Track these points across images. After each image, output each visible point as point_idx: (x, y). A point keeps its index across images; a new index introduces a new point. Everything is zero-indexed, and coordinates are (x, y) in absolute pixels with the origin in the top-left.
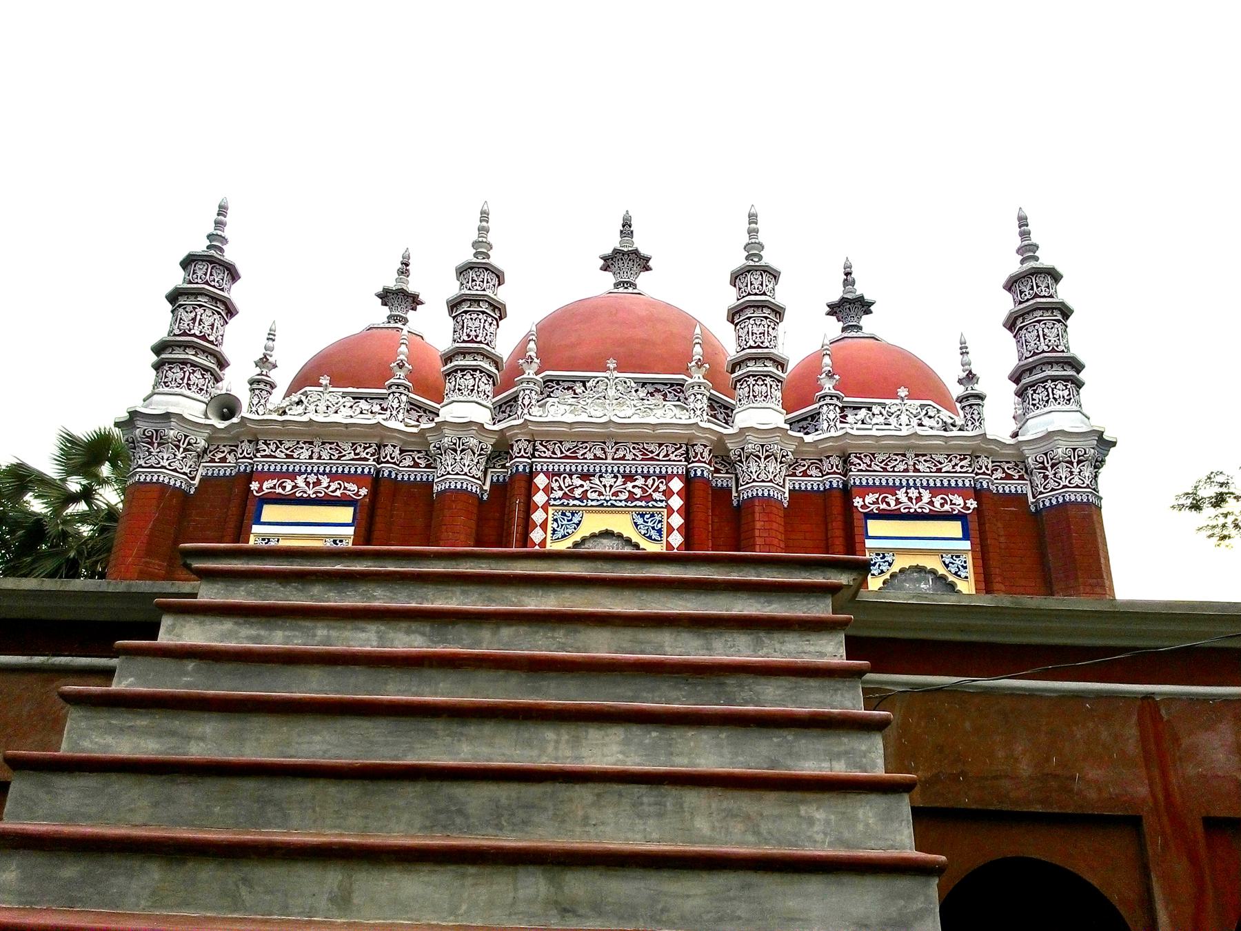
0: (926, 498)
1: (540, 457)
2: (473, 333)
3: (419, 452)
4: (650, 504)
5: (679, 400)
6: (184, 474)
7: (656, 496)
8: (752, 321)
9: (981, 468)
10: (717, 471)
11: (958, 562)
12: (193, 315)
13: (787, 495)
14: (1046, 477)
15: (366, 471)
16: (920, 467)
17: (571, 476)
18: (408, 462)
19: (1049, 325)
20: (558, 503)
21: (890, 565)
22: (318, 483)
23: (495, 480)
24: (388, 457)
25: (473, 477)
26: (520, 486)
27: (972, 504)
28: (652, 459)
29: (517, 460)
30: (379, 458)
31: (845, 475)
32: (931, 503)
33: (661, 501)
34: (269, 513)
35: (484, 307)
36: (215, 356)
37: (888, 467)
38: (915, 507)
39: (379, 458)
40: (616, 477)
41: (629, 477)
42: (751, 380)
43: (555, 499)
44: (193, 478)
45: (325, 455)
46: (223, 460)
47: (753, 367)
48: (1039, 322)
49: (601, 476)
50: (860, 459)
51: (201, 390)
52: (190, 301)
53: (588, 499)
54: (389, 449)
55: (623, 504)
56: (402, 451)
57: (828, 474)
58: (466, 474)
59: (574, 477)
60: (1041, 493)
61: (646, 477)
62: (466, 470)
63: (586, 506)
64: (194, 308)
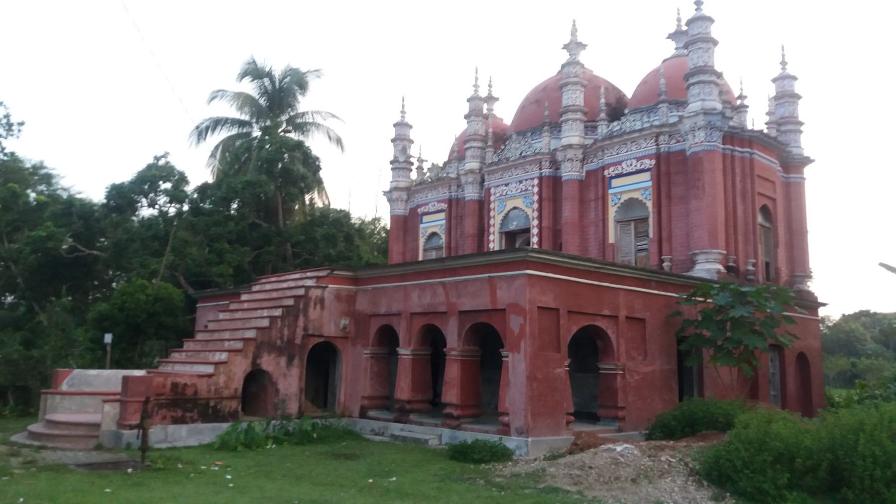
0: (634, 165)
4: (527, 192)
7: (530, 188)
11: (647, 192)
21: (620, 199)
22: (434, 205)
27: (653, 162)
28: (527, 172)
32: (636, 166)
34: (426, 218)
38: (630, 170)
40: (516, 183)
41: (521, 182)
54: (452, 187)
61: (526, 180)
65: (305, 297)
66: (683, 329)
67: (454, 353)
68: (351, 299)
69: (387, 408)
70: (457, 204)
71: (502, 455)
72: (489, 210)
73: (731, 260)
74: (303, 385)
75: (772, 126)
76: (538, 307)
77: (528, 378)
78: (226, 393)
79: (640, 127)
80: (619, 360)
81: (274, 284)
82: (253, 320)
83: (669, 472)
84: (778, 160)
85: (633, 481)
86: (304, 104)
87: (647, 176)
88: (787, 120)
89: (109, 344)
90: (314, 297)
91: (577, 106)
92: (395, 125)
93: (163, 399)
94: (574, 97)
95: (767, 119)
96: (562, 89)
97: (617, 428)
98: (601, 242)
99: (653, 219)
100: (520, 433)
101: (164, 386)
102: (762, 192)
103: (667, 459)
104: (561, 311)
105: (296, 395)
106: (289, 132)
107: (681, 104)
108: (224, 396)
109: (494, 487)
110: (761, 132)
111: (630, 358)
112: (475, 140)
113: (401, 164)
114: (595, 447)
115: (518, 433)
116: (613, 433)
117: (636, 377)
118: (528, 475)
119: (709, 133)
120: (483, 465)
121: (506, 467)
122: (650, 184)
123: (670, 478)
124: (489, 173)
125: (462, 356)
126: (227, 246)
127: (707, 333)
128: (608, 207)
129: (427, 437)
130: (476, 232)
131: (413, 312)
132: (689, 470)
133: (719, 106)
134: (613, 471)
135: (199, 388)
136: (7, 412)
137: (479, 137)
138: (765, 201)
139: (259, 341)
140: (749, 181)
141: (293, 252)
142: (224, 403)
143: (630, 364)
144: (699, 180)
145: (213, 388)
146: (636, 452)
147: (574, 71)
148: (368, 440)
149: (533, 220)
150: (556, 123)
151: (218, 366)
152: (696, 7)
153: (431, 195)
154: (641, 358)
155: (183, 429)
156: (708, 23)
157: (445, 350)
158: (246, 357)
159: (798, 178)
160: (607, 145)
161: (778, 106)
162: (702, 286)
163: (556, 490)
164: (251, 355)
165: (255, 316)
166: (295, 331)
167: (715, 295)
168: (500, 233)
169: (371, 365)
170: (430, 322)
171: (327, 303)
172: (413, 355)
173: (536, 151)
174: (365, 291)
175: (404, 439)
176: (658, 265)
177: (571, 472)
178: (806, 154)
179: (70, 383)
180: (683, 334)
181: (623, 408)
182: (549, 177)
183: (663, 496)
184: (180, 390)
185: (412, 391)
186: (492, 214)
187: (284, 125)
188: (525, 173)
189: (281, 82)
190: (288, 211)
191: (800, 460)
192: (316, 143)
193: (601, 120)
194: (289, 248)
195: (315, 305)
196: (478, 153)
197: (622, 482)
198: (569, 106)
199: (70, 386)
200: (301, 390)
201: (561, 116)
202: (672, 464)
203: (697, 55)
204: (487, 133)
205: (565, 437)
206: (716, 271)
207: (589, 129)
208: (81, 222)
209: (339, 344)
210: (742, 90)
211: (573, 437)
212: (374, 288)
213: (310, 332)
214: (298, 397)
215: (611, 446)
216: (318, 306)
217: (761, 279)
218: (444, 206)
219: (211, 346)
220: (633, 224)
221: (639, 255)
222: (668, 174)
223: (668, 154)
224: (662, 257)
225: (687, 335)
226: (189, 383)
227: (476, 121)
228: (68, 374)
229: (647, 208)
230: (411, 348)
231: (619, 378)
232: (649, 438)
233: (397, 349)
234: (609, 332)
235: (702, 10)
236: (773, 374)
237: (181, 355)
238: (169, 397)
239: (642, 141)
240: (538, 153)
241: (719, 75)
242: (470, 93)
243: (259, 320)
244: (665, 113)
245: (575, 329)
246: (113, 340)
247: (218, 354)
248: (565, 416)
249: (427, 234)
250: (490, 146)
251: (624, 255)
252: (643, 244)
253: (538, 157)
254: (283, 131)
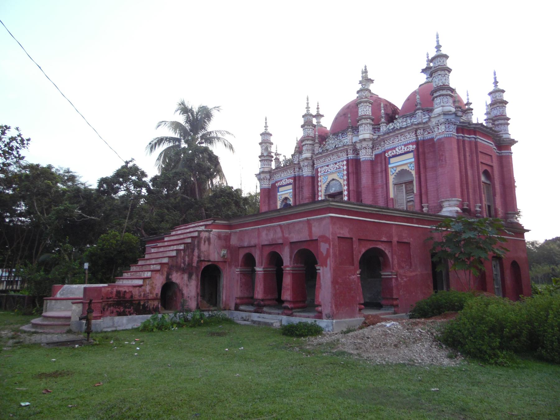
7: (342, 167)
11: (412, 165)
16: (402, 139)
17: (325, 166)
21: (395, 171)
22: (286, 181)
27: (414, 146)
28: (340, 157)
32: (404, 150)
34: (281, 189)
38: (400, 152)
41: (336, 163)
50: (387, 141)
54: (296, 169)
61: (339, 162)
65: (198, 237)
66: (434, 248)
67: (288, 269)
68: (227, 238)
69: (252, 305)
71: (316, 331)
72: (318, 182)
73: (465, 205)
74: (199, 291)
75: (489, 121)
76: (338, 237)
77: (332, 282)
78: (151, 296)
79: (406, 126)
80: (393, 269)
81: (183, 230)
82: (168, 252)
83: (420, 340)
84: (493, 142)
85: (396, 346)
86: (211, 127)
87: (411, 155)
88: (498, 117)
89: (87, 269)
90: (204, 237)
91: (368, 115)
92: (261, 135)
93: (111, 301)
94: (365, 110)
95: (485, 117)
96: (358, 106)
97: (393, 311)
98: (386, 198)
99: (416, 181)
100: (328, 317)
101: (112, 293)
102: (483, 162)
103: (419, 331)
104: (354, 239)
105: (195, 297)
106: (202, 143)
107: (430, 111)
108: (149, 298)
109: (304, 352)
110: (482, 124)
111: (401, 267)
112: (308, 140)
113: (266, 157)
114: (373, 324)
115: (327, 317)
116: (390, 315)
117: (405, 279)
118: (327, 344)
119: (447, 126)
120: (302, 338)
121: (316, 339)
122: (413, 160)
123: (420, 343)
124: (317, 159)
125: (292, 271)
126: (166, 211)
127: (449, 250)
128: (388, 176)
129: (272, 322)
130: (311, 196)
131: (263, 244)
132: (433, 337)
133: (453, 110)
134: (382, 340)
135: (134, 293)
136: (34, 311)
137: (310, 138)
138: (486, 168)
139: (170, 265)
140: (474, 155)
141: (206, 213)
142: (150, 302)
143: (401, 271)
144: (442, 155)
145: (142, 294)
146: (399, 327)
147: (364, 95)
148: (237, 324)
149: (344, 186)
150: (356, 127)
151: (145, 280)
152: (436, 50)
153: (284, 175)
154: (408, 267)
155: (124, 319)
156: (444, 58)
157: (282, 267)
158: (162, 274)
159: (507, 153)
160: (387, 137)
161: (493, 109)
162: (446, 221)
163: (343, 353)
164: (165, 273)
165: (170, 249)
166: (192, 259)
167: (452, 225)
168: (324, 195)
169: (241, 278)
170: (273, 250)
171: (212, 241)
172: (264, 271)
173: (345, 144)
174: (236, 232)
175: (259, 323)
176: (420, 210)
177: (356, 341)
178: (512, 137)
179: (62, 293)
180: (434, 251)
181: (396, 299)
182: (352, 160)
183: (414, 356)
184: (122, 295)
185: (264, 293)
186: (319, 184)
187: (199, 140)
189: (197, 114)
190: (202, 190)
191: (507, 330)
192: (217, 149)
193: (382, 123)
194: (204, 211)
195: (205, 242)
196: (310, 147)
197: (388, 347)
198: (363, 115)
199: (62, 295)
200: (198, 294)
201: (358, 122)
202: (423, 334)
203: (438, 79)
204: (315, 135)
205: (359, 318)
206: (456, 211)
207: (376, 129)
208: (85, 201)
209: (220, 266)
210: (468, 99)
211: (364, 318)
212: (240, 231)
213: (202, 259)
214: (196, 298)
215: (383, 323)
216: (207, 243)
217: (485, 216)
218: (291, 181)
219: (144, 268)
220: (404, 185)
221: (408, 204)
222: (424, 153)
223: (424, 141)
224: (422, 205)
225: (437, 252)
226: (127, 291)
227: (308, 128)
228: (61, 287)
229: (412, 174)
230: (263, 266)
231: (394, 280)
232: (411, 317)
233: (255, 268)
234: (387, 252)
235: (441, 51)
236: (496, 275)
237: (127, 274)
238: (115, 300)
239: (407, 134)
240: (345, 145)
241: (453, 90)
242: (304, 112)
243: (171, 252)
244: (420, 116)
245: (363, 251)
246: (89, 267)
247: (146, 273)
248: (358, 306)
249: (282, 199)
250: (317, 143)
251: (400, 205)
252: (411, 197)
253: (346, 147)
254: (199, 143)
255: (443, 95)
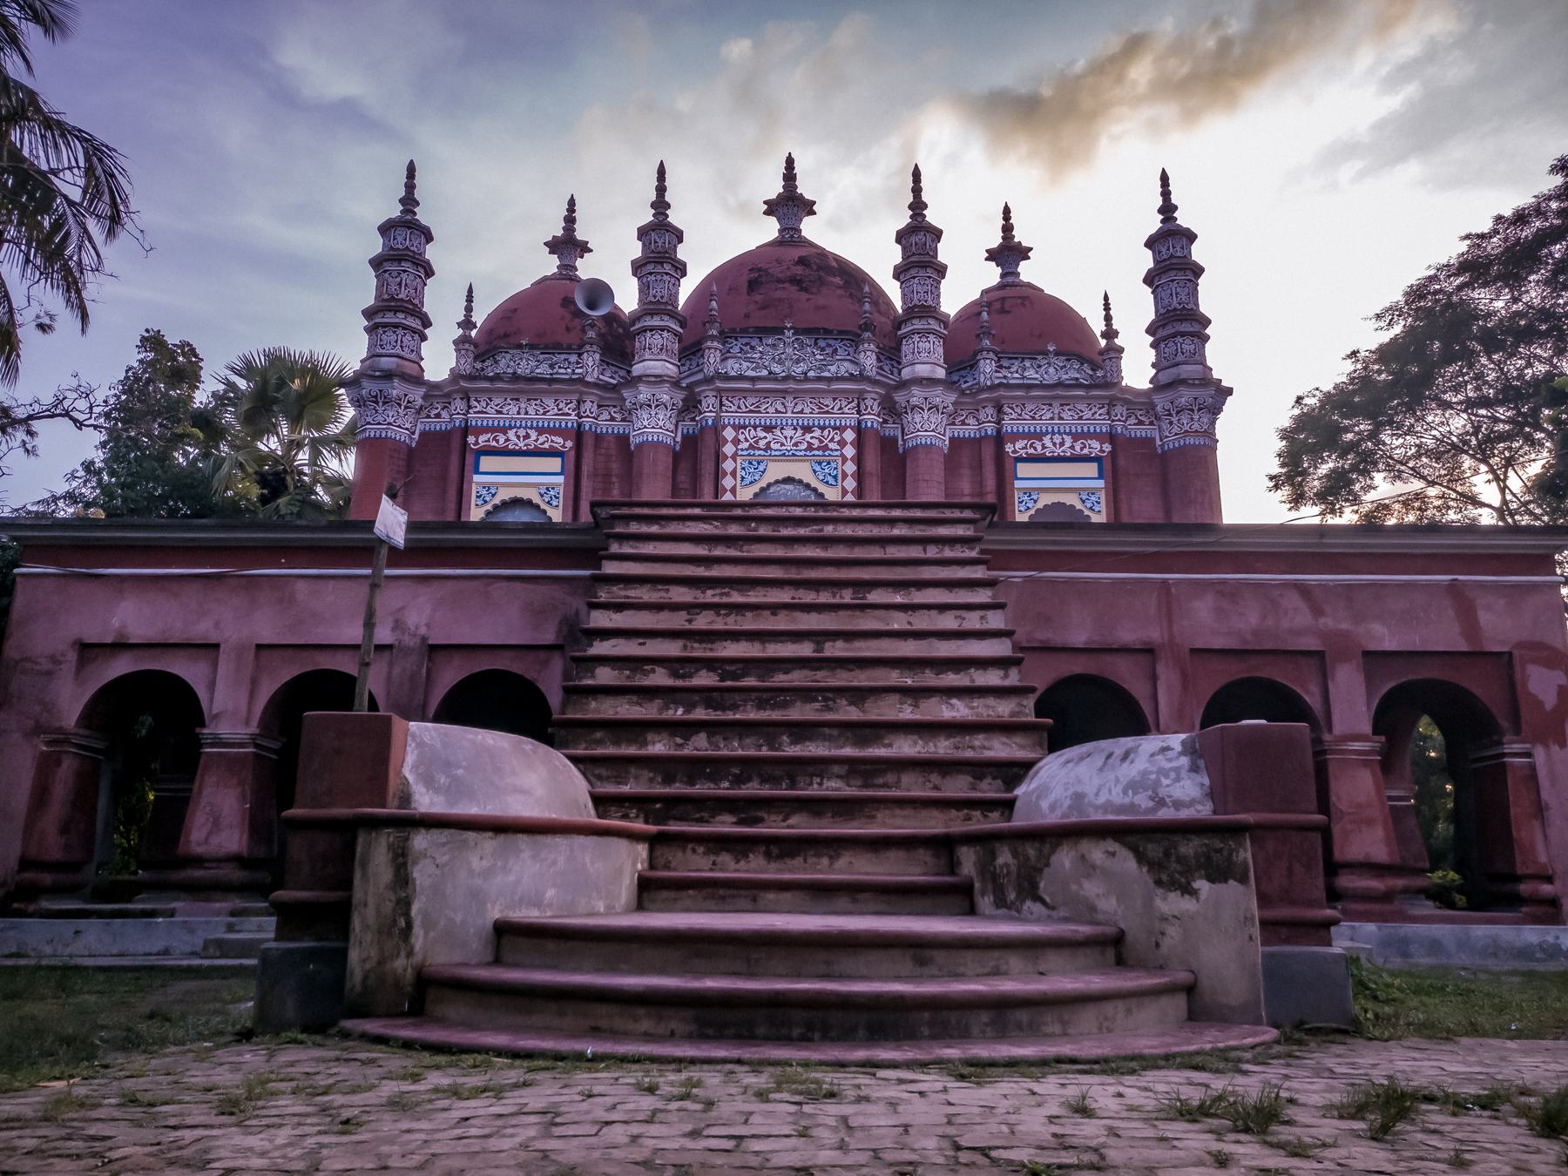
0: (1068, 444)
1: (727, 412)
2: (659, 294)
3: (615, 407)
4: (826, 453)
5: (849, 355)
6: (407, 429)
7: (831, 446)
8: (916, 280)
9: (1116, 416)
10: (885, 421)
11: (1093, 498)
12: (398, 279)
13: (947, 442)
14: (1171, 423)
15: (570, 425)
17: (755, 427)
18: (605, 416)
19: (1182, 284)
20: (745, 453)
21: (1035, 502)
23: (685, 432)
24: (588, 412)
25: (667, 430)
26: (709, 439)
27: (1107, 447)
28: (827, 412)
29: (707, 414)
30: (579, 413)
31: (998, 423)
32: (1072, 447)
33: (836, 450)
34: (487, 463)
35: (667, 267)
36: (421, 319)
37: (1036, 416)
38: (1058, 451)
39: (579, 413)
40: (795, 429)
41: (807, 429)
42: (916, 338)
43: (742, 450)
44: (413, 433)
45: (531, 411)
46: (438, 416)
47: (918, 324)
48: (1173, 281)
49: (782, 429)
50: (1012, 409)
51: (412, 351)
52: (394, 267)
53: (771, 449)
54: (588, 405)
55: (803, 453)
56: (599, 406)
57: (984, 422)
58: (661, 428)
59: (759, 429)
60: (1167, 437)
61: (823, 428)
62: (661, 423)
63: (770, 455)
64: (399, 274)
67: (1356, 746)
70: (597, 446)
188: (819, 413)
239: (1082, 407)
249: (497, 501)
255: (1183, 334)
